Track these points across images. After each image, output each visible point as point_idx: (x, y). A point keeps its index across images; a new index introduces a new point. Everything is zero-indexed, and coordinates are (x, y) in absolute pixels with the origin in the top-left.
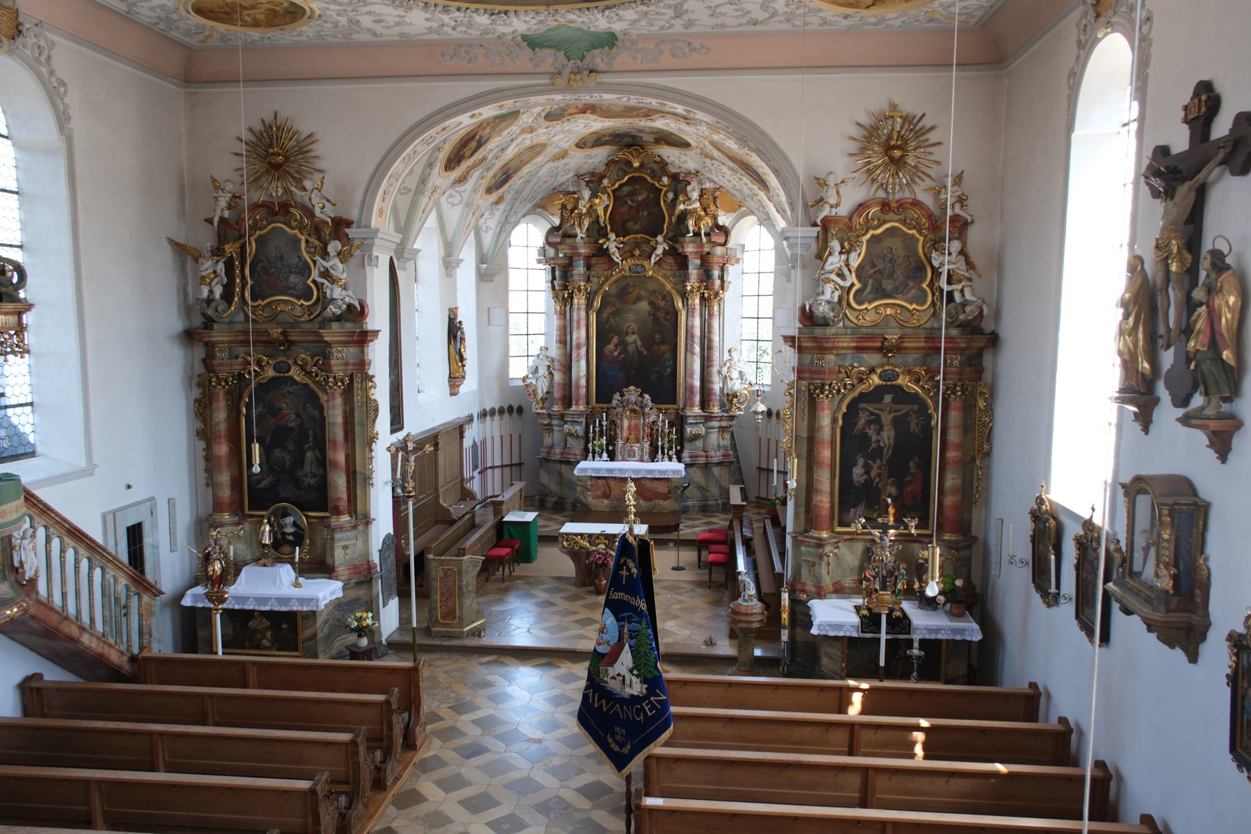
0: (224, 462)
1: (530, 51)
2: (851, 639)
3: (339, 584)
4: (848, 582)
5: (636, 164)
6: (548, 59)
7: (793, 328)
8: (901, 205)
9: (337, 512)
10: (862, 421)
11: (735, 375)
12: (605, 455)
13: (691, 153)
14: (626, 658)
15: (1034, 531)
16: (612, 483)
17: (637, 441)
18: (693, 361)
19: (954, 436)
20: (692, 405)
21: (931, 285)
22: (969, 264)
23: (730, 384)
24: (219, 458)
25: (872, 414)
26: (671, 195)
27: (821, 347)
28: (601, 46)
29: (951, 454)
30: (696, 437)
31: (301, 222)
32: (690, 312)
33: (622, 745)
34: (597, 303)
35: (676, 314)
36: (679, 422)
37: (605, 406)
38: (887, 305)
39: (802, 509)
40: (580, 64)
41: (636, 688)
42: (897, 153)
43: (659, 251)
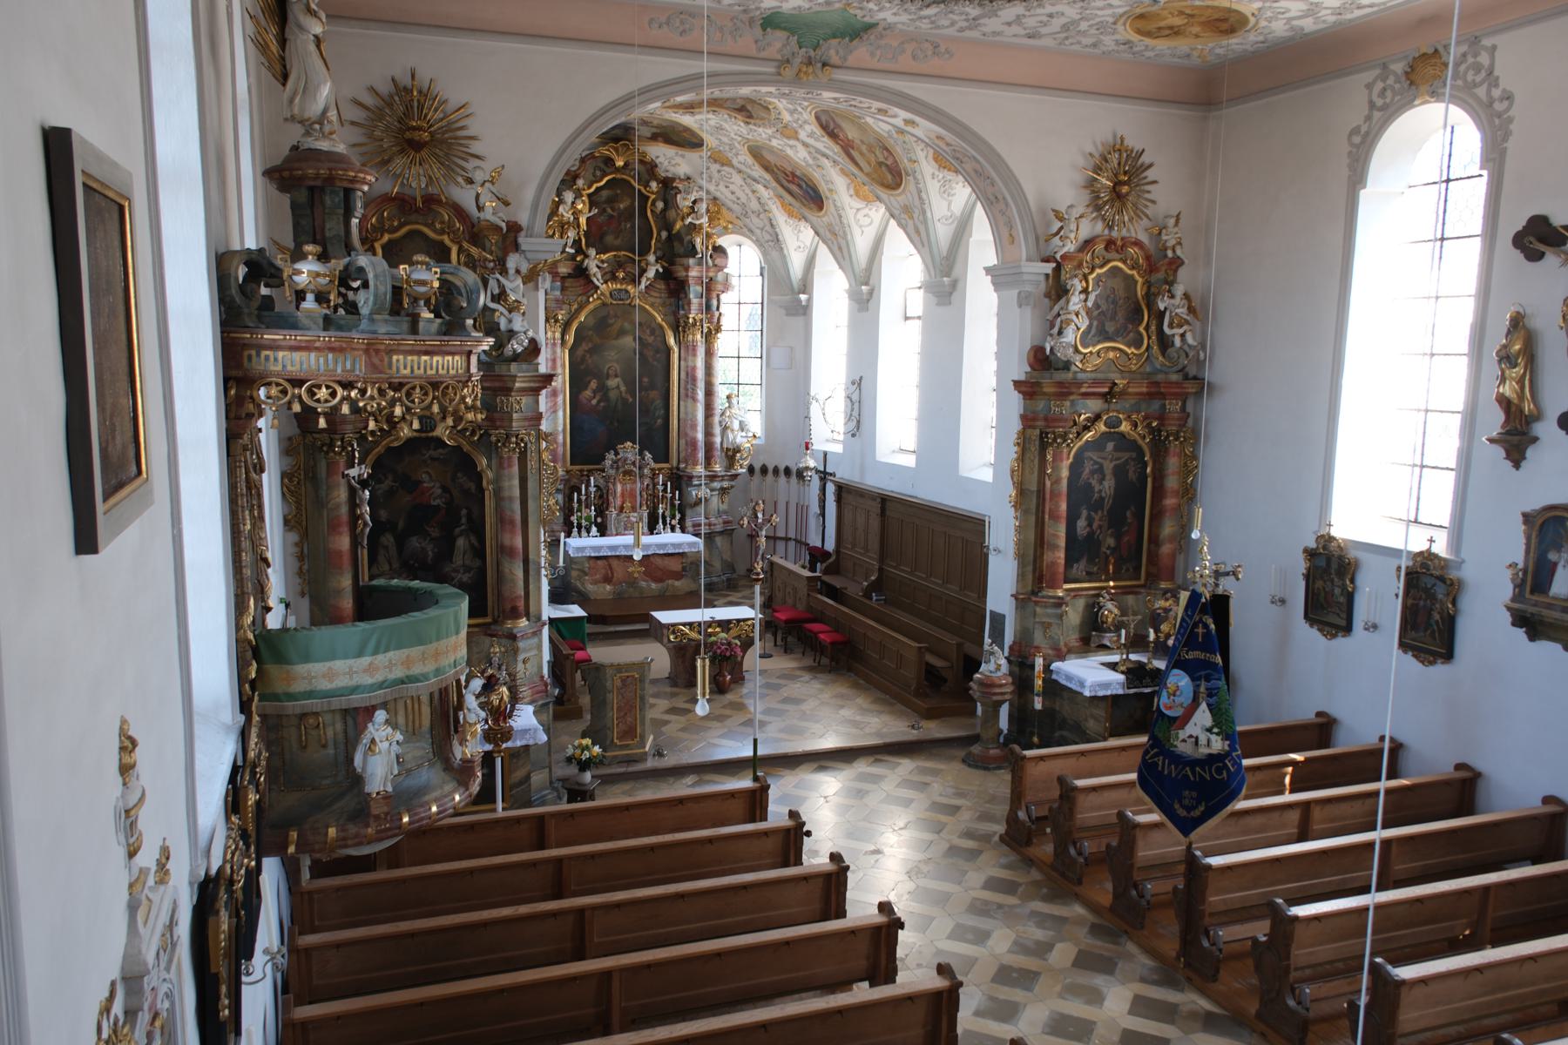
0: (346, 560)
1: (758, 31)
2: (1115, 697)
3: (531, 709)
4: (1073, 638)
5: (620, 163)
6: (778, 39)
7: (1020, 370)
8: (1126, 242)
9: (515, 614)
10: (1087, 471)
11: (736, 425)
12: (594, 529)
13: (693, 155)
14: (1203, 717)
15: (1309, 570)
16: (615, 563)
17: (634, 509)
18: (695, 410)
19: (1172, 482)
20: (695, 463)
21: (1147, 328)
22: (1191, 310)
23: (731, 436)
24: (339, 554)
25: (1096, 463)
26: (660, 205)
27: (1065, 391)
28: (843, 36)
29: (1170, 502)
30: (698, 502)
31: (450, 225)
32: (688, 349)
33: (1189, 809)
34: (570, 338)
35: (668, 350)
36: (680, 480)
37: (586, 467)
38: (1108, 349)
39: (1030, 568)
40: (812, 53)
41: (1218, 745)
42: (1125, 189)
43: (651, 273)
